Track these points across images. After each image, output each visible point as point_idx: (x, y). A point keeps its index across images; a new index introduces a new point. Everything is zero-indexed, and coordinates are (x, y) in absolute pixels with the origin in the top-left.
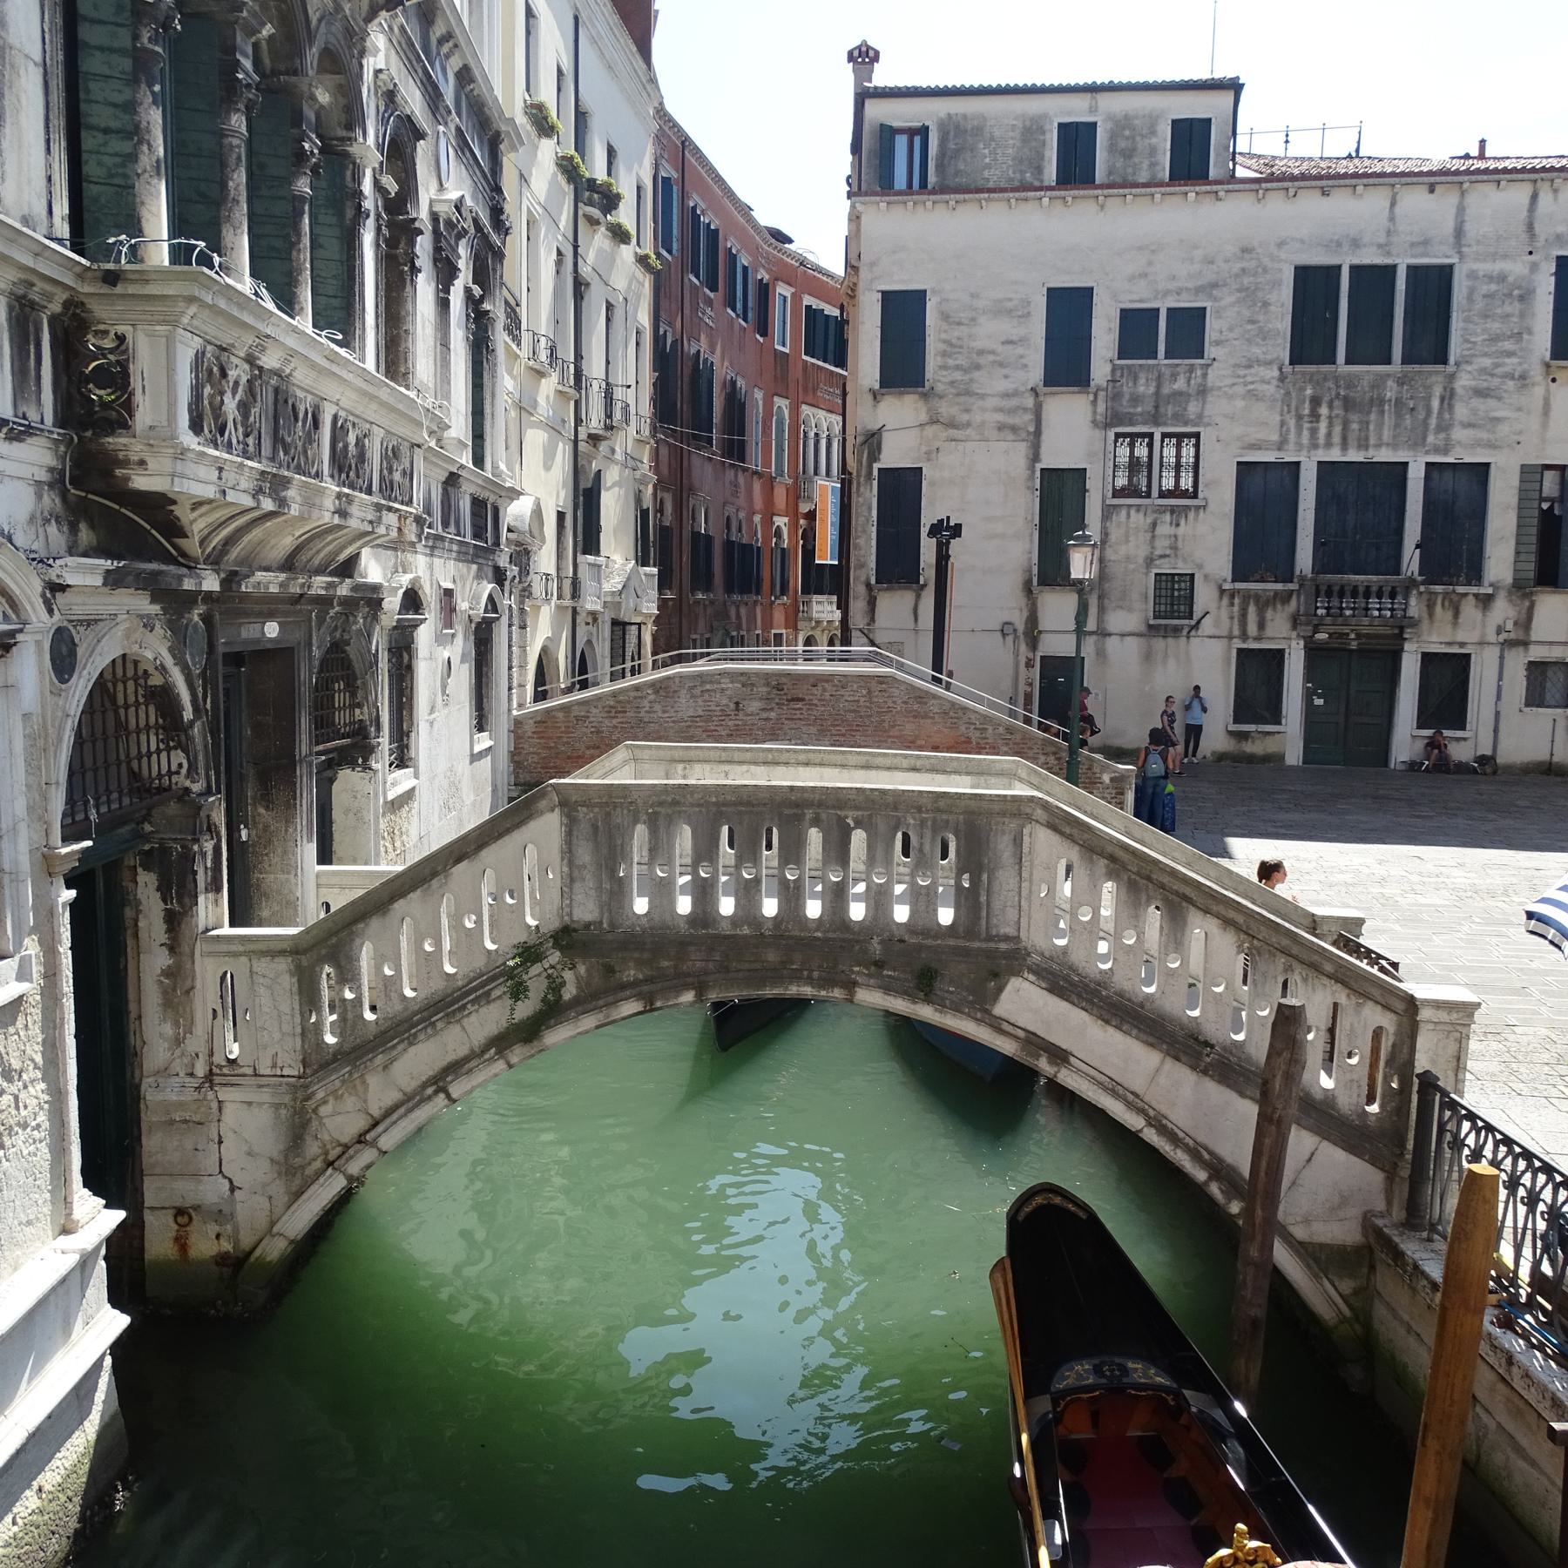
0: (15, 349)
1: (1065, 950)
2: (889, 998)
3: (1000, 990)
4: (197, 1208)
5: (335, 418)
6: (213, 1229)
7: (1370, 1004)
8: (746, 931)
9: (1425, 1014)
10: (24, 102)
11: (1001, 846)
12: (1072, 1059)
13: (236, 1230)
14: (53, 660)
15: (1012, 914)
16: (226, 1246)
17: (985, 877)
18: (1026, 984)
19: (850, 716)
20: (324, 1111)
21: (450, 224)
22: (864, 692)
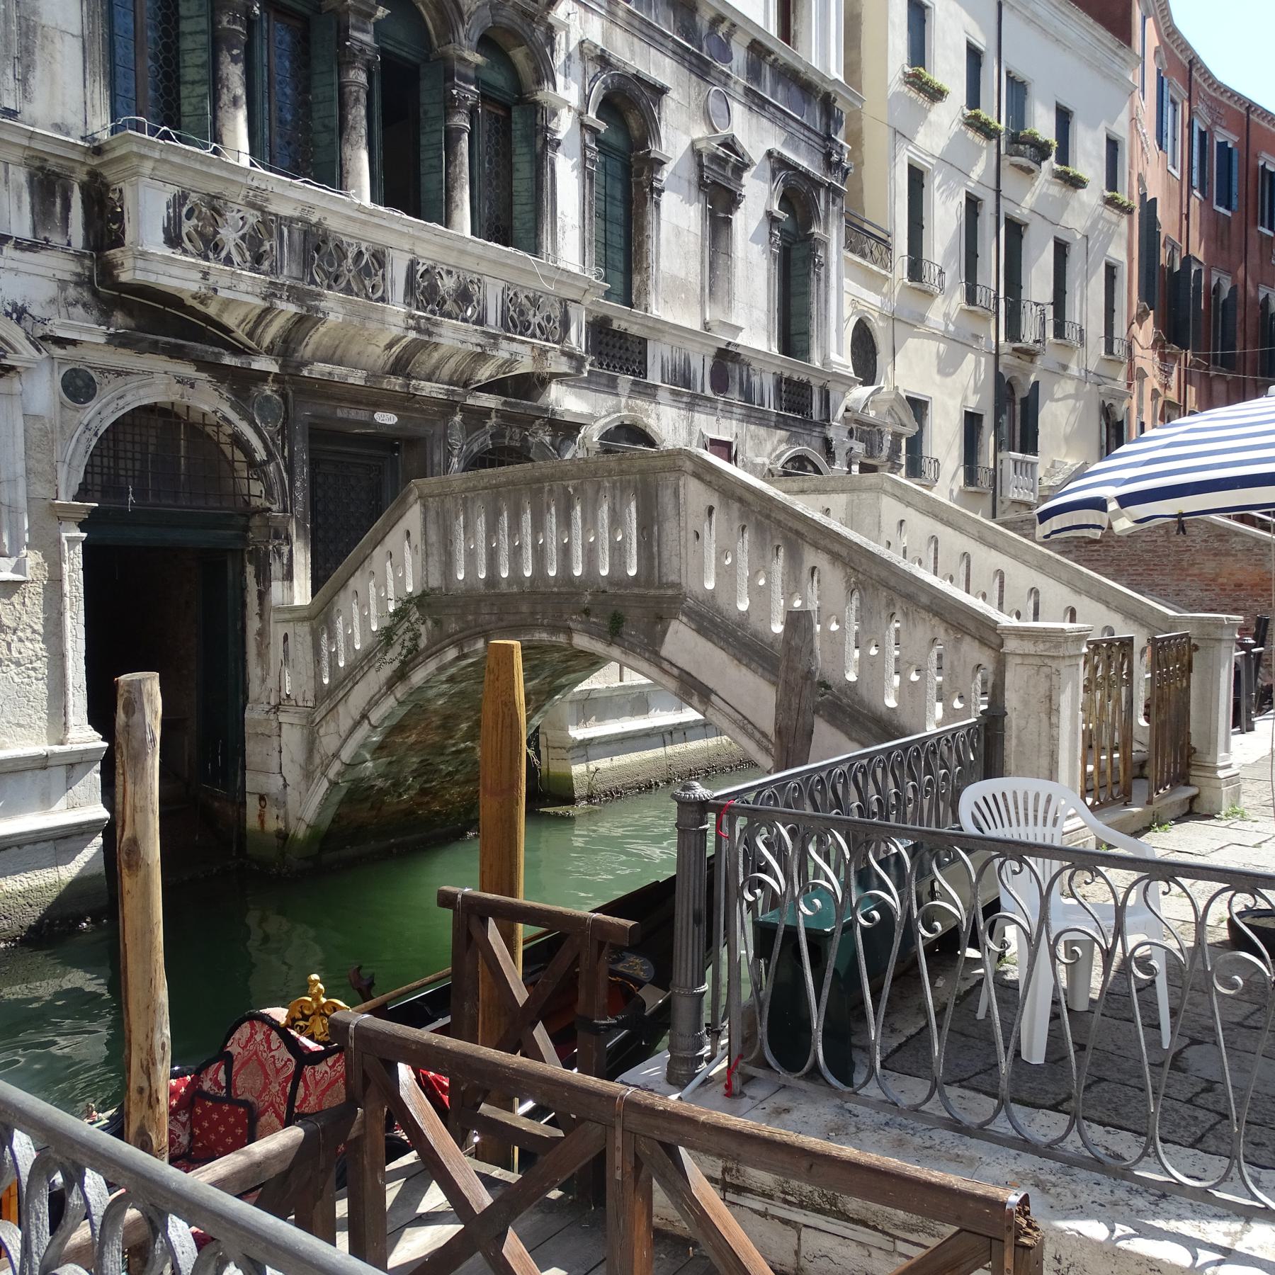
0: (37, 200)
1: (713, 594)
2: (594, 642)
3: (665, 632)
4: (267, 795)
5: (412, 266)
6: (274, 811)
7: (968, 639)
8: (515, 589)
9: (1011, 645)
10: (58, 56)
11: (666, 499)
12: (713, 697)
13: (286, 813)
14: (65, 388)
15: (675, 560)
16: (281, 825)
17: (656, 528)
18: (682, 627)
19: (1147, 556)
20: (322, 731)
21: (715, 158)
22: (1162, 532)
